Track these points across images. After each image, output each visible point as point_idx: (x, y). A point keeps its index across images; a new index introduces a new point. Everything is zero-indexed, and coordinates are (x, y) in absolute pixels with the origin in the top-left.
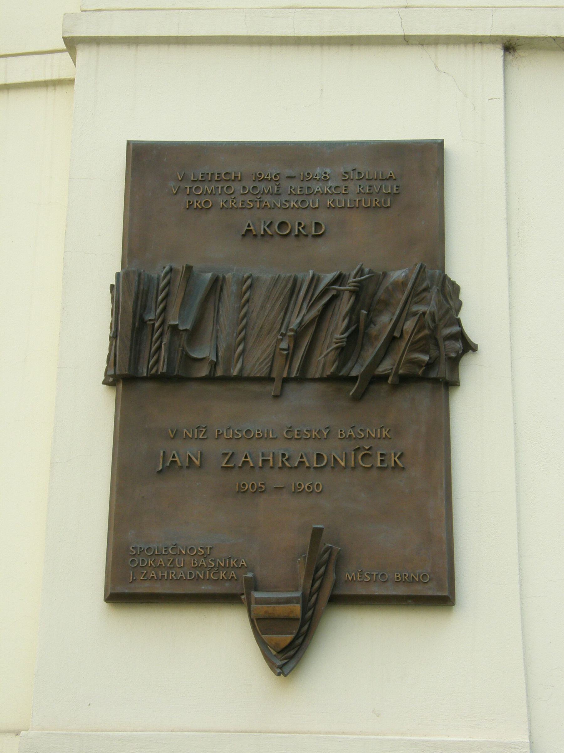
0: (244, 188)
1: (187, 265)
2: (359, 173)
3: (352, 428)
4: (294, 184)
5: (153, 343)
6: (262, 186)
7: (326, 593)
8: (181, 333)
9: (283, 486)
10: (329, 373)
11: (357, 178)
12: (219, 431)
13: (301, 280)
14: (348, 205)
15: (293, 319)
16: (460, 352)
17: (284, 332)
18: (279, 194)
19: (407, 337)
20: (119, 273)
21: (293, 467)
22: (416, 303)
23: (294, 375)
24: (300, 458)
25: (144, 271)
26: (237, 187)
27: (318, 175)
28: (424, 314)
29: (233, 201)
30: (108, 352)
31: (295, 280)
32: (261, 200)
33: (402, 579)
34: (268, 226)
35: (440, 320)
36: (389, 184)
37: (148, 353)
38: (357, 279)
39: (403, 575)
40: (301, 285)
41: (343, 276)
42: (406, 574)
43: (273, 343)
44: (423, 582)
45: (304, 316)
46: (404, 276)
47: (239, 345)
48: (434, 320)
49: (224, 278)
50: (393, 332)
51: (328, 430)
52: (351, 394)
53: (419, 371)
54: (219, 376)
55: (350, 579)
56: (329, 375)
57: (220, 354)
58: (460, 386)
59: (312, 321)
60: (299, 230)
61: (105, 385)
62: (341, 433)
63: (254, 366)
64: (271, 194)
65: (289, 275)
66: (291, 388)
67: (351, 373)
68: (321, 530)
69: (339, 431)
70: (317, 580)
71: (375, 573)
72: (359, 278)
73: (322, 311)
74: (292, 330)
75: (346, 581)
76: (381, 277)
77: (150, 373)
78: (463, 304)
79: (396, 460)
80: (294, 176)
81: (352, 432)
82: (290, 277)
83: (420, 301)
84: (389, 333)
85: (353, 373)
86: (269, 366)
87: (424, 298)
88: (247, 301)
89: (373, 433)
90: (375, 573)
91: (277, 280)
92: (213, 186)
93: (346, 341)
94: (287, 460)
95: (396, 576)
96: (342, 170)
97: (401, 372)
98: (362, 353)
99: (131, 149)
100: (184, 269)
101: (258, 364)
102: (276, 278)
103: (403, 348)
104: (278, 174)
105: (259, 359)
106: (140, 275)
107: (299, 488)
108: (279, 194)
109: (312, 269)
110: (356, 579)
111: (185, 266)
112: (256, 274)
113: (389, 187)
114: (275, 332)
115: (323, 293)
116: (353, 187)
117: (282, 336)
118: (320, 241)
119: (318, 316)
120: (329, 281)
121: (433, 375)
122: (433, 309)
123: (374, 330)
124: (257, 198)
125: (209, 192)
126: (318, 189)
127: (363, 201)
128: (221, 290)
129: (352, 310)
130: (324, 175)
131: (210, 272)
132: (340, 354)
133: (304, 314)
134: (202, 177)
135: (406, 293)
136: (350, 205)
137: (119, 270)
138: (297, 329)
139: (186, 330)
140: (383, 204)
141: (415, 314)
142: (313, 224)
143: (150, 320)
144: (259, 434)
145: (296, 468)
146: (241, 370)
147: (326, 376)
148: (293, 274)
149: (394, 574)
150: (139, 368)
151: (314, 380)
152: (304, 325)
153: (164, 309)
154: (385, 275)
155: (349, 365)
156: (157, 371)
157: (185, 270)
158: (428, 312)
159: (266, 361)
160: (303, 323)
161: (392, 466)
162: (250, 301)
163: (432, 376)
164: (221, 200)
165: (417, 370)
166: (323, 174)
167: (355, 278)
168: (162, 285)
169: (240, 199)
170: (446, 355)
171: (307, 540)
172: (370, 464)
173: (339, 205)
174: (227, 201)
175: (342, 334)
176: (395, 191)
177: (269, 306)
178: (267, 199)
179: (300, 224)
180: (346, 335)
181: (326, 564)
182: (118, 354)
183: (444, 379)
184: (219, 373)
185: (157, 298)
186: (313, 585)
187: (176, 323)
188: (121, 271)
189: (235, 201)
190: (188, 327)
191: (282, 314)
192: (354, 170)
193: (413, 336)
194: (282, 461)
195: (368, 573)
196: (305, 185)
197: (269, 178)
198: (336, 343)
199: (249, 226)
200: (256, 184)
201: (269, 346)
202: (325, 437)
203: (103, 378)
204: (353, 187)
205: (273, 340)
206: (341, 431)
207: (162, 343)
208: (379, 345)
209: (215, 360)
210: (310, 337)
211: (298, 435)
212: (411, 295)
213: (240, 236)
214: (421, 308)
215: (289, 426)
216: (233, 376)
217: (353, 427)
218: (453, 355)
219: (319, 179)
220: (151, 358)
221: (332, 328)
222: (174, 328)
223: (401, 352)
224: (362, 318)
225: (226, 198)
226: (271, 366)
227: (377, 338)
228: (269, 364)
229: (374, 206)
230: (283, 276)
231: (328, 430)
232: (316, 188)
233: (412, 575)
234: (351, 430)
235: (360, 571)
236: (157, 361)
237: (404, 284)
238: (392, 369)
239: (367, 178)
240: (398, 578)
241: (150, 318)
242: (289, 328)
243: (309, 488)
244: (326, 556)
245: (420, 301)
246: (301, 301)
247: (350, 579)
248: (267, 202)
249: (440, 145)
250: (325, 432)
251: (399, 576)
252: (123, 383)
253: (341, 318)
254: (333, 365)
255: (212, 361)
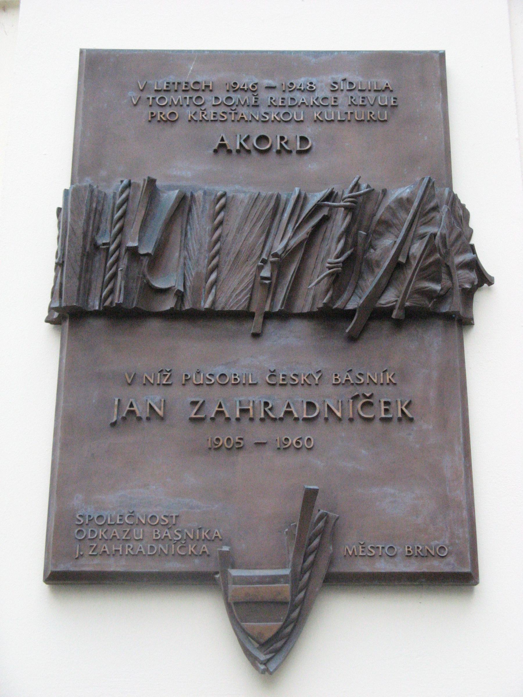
0: (217, 98)
1: (149, 178)
2: (351, 83)
3: (348, 372)
4: (276, 95)
5: (107, 270)
6: (236, 97)
7: (322, 570)
8: (142, 258)
9: (266, 441)
10: (321, 305)
11: (348, 88)
12: (186, 375)
13: (285, 199)
14: (338, 118)
15: (276, 243)
16: (476, 283)
17: (266, 259)
18: (257, 106)
19: (414, 263)
20: (68, 190)
21: (278, 418)
22: (425, 224)
23: (278, 308)
24: (287, 408)
25: (98, 187)
26: (208, 98)
27: (302, 85)
28: (435, 235)
29: (203, 113)
30: (52, 285)
31: (278, 199)
32: (236, 112)
33: (414, 552)
34: (246, 140)
35: (452, 245)
36: (385, 95)
37: (102, 280)
38: (354, 194)
39: (416, 548)
40: (286, 204)
41: (335, 194)
42: (419, 546)
43: (252, 271)
44: (439, 556)
45: (290, 239)
46: (408, 192)
47: (212, 272)
48: (445, 245)
49: (192, 196)
50: (398, 257)
51: (320, 374)
52: (347, 331)
53: (430, 303)
54: (188, 310)
55: (350, 553)
56: (321, 308)
57: (188, 284)
58: (475, 327)
59: (300, 245)
60: (281, 144)
61: (48, 324)
62: (336, 377)
63: (231, 297)
64: (248, 106)
65: (270, 193)
66: (272, 326)
67: (347, 306)
68: (315, 492)
69: (334, 375)
70: (310, 554)
71: (380, 546)
72: (355, 192)
73: (311, 233)
74: (275, 255)
75: (345, 556)
76: (380, 197)
77: (103, 304)
78: (474, 230)
79: (404, 409)
80: (274, 86)
81: (349, 377)
82: (272, 196)
83: (429, 221)
84: (393, 256)
85: (350, 306)
86: (248, 298)
87: (433, 218)
88: (221, 223)
89: (375, 378)
90: (380, 546)
91: (257, 198)
92: (180, 97)
93: (342, 266)
94: (270, 409)
95: (407, 549)
96: (330, 81)
97: (407, 304)
98: (360, 282)
99: (85, 57)
100: (146, 182)
101: (234, 295)
102: (256, 197)
103: (410, 276)
104: (256, 84)
105: (235, 289)
106: (92, 191)
107: (286, 443)
108: (257, 106)
109: (298, 187)
110: (358, 552)
111: (147, 179)
112: (230, 190)
113: (385, 99)
114: (254, 259)
115: (312, 213)
116: (343, 99)
117: (264, 264)
118: (306, 157)
119: (306, 239)
120: (319, 199)
121: (445, 308)
122: (444, 232)
123: (374, 254)
124: (232, 110)
125: (176, 103)
126: (303, 100)
127: (356, 114)
128: (190, 210)
129: (347, 231)
130: (310, 85)
131: (176, 189)
132: (334, 282)
133: (289, 238)
134: (167, 87)
135: (412, 211)
136: (341, 117)
137: (68, 186)
138: (281, 255)
139: (147, 255)
140: (379, 117)
141: (422, 236)
142: (298, 139)
143: (104, 244)
144: (236, 379)
145: (281, 419)
146: (214, 302)
147: (317, 310)
148: (276, 193)
149: (405, 547)
150: (90, 301)
151: (302, 316)
152: (290, 250)
153: (121, 230)
154: (385, 192)
155: (345, 296)
156: (111, 303)
157: (147, 184)
158: (439, 234)
159: (245, 292)
160: (289, 248)
161: (398, 417)
162: (225, 223)
163: (444, 311)
164: (190, 112)
165: (427, 302)
166: (308, 84)
167: (351, 192)
168: (119, 201)
169: (212, 110)
170: (460, 286)
171: (298, 504)
172: (372, 415)
173: (327, 117)
174: (196, 112)
175: (337, 257)
176: (393, 104)
177: (247, 229)
178: (245, 111)
179: (282, 138)
180: (341, 259)
181: (320, 535)
182: (64, 283)
183: (457, 313)
184: (187, 306)
185: (113, 216)
186: (304, 561)
187: (136, 244)
188: (71, 187)
189: (205, 113)
190: (150, 250)
191: (263, 238)
192: (344, 80)
193: (422, 261)
194: (265, 411)
195: (373, 546)
196: (287, 95)
197: (246, 88)
198: (330, 268)
199: (222, 140)
200: (231, 94)
201: (246, 275)
202: (317, 383)
203: (46, 314)
204: (343, 99)
205: (251, 269)
206: (336, 375)
207: (118, 269)
208: (380, 272)
209: (182, 289)
210: (297, 263)
211: (283, 380)
212: (418, 214)
213: (211, 152)
214: (431, 230)
215: (272, 370)
216: (204, 310)
217: (350, 371)
218: (467, 286)
219: (304, 89)
220: (104, 287)
221: (323, 255)
222: (133, 252)
223: (407, 281)
224: (360, 240)
225: (194, 109)
226: (251, 299)
227: (378, 264)
228: (249, 296)
229: (369, 119)
230: (263, 194)
231: (320, 374)
232: (300, 99)
233: (427, 547)
234: (348, 374)
235: (362, 543)
236: (112, 292)
237: (409, 201)
238: (396, 301)
239: (360, 88)
240: (409, 552)
241: (104, 242)
242: (272, 253)
243: (298, 443)
244: (321, 524)
245: (429, 221)
246: (286, 222)
247: (350, 553)
248: (243, 114)
249: (442, 56)
250: (317, 376)
251: (410, 549)
252: (69, 321)
253: (335, 240)
254: (326, 295)
255: (179, 291)
